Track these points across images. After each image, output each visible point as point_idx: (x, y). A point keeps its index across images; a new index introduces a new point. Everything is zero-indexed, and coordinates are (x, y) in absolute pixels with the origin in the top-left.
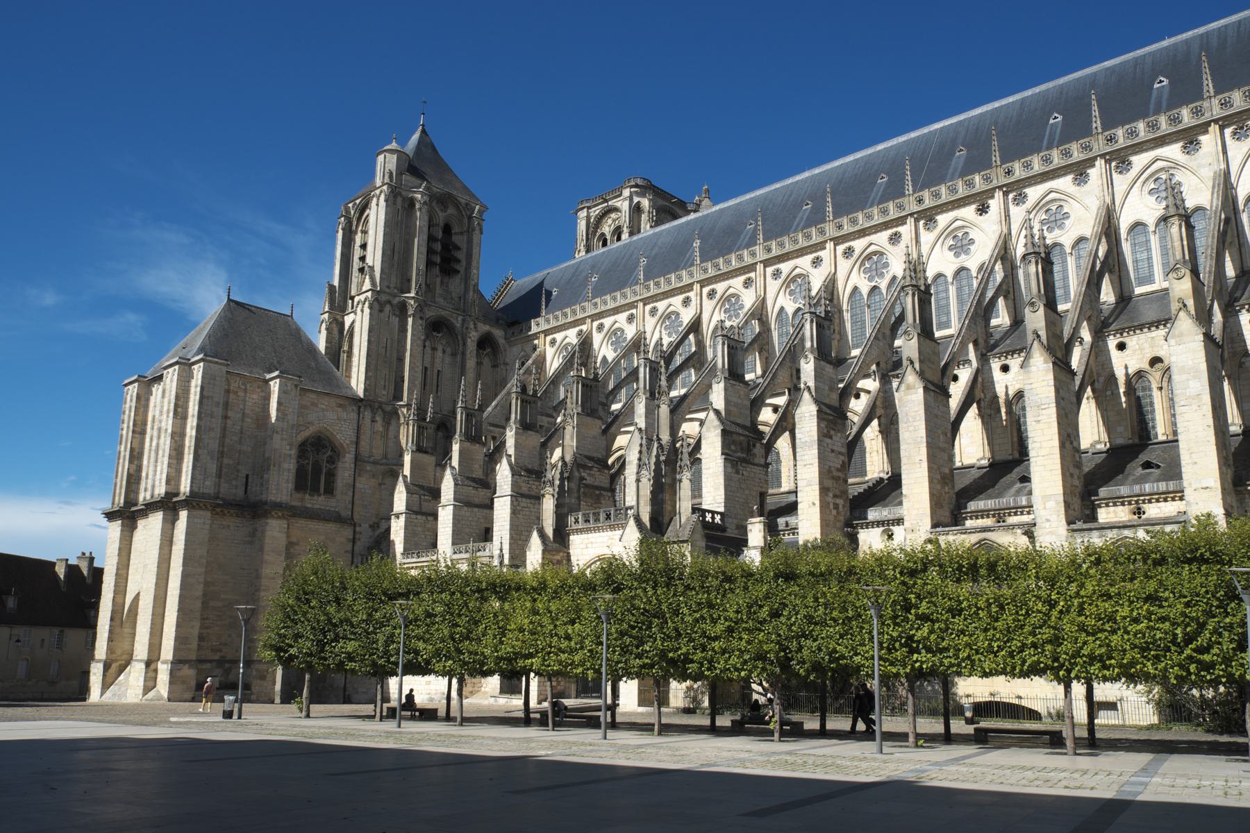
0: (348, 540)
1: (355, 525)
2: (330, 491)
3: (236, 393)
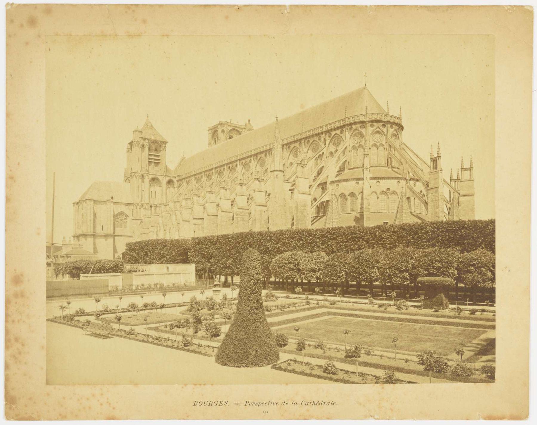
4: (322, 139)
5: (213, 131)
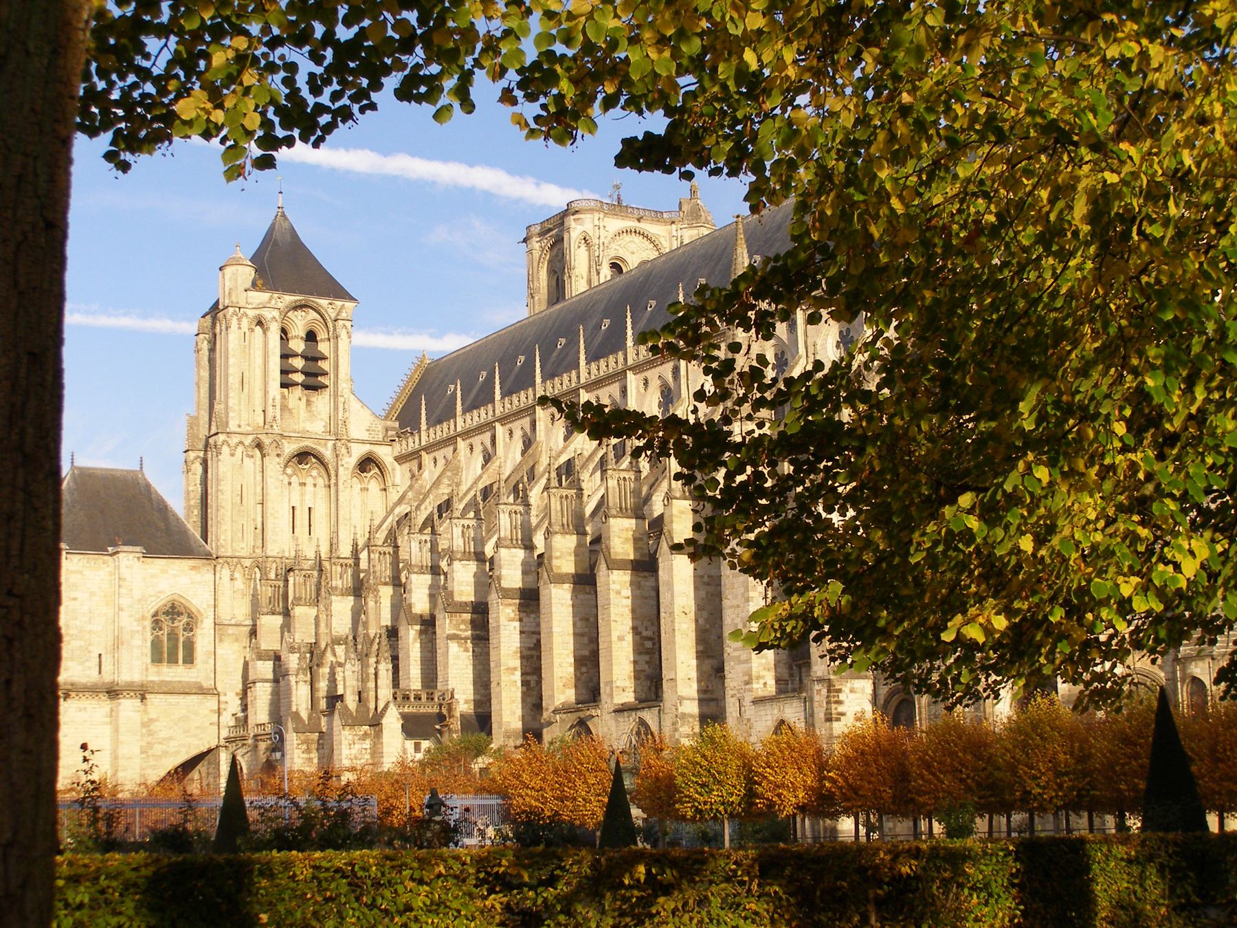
0: (212, 711)
1: (218, 694)
2: (189, 659)
3: (81, 573)
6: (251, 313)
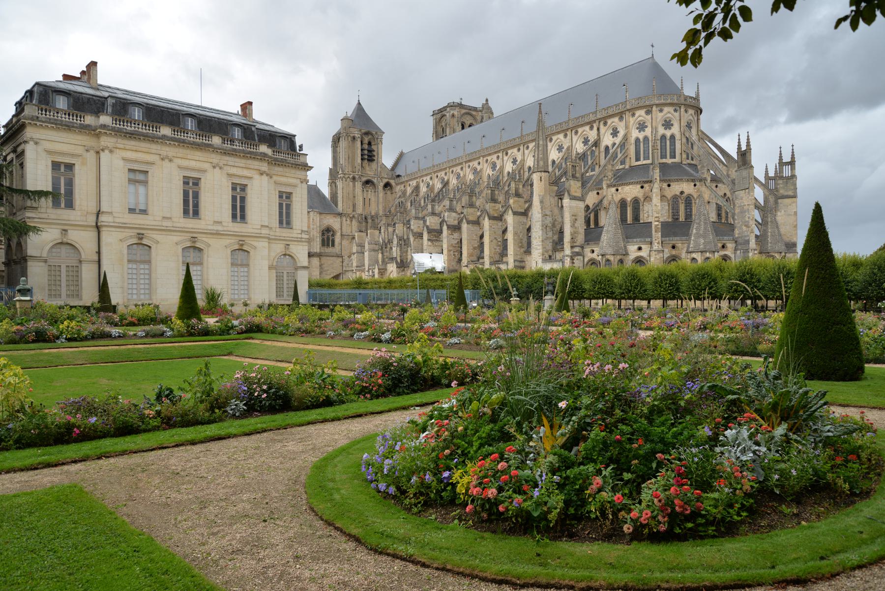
2: (333, 245)
4: (595, 128)
5: (439, 116)
6: (352, 135)
